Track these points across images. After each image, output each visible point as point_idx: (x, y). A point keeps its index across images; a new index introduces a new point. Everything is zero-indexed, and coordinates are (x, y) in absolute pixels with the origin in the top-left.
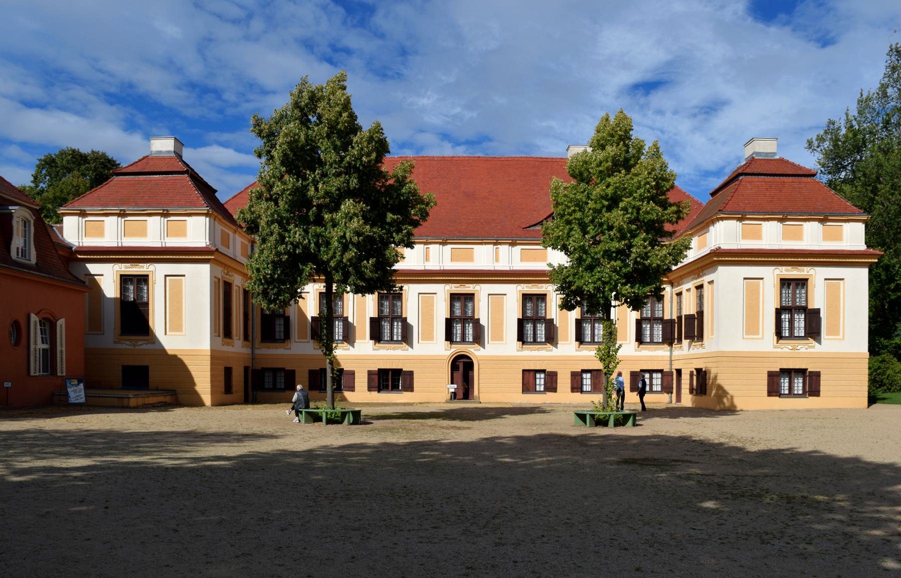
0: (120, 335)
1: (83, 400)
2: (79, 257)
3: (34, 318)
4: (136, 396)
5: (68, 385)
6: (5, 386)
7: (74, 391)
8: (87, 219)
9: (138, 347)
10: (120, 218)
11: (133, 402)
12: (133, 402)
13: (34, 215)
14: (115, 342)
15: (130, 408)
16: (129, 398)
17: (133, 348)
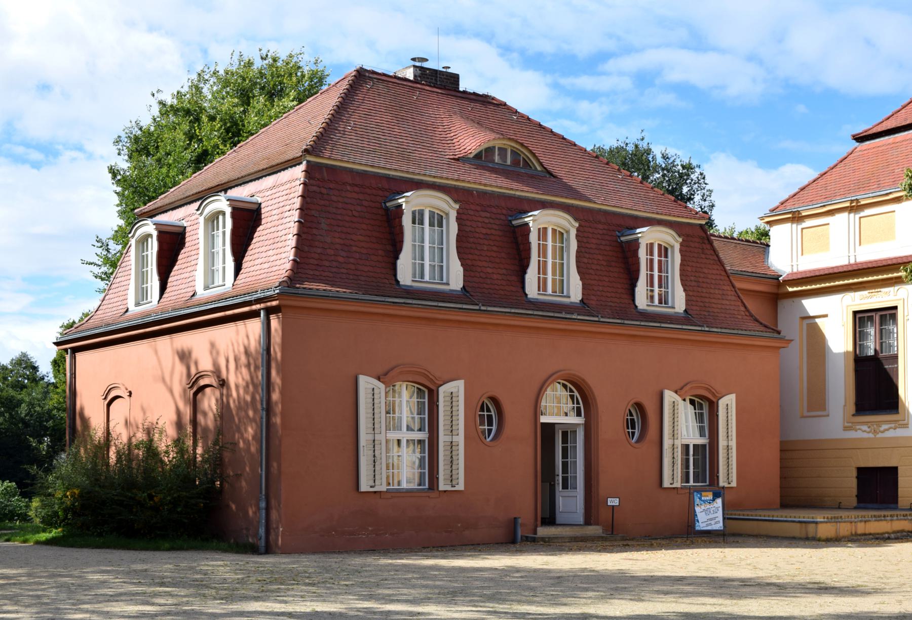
0: (853, 415)
1: (719, 526)
2: (790, 289)
3: (669, 396)
4: (835, 520)
5: (697, 501)
6: (609, 504)
7: (706, 511)
8: (804, 225)
9: (880, 435)
10: (852, 215)
11: (825, 530)
12: (825, 530)
13: (680, 236)
14: (846, 429)
15: (819, 540)
16: (816, 523)
17: (871, 435)
